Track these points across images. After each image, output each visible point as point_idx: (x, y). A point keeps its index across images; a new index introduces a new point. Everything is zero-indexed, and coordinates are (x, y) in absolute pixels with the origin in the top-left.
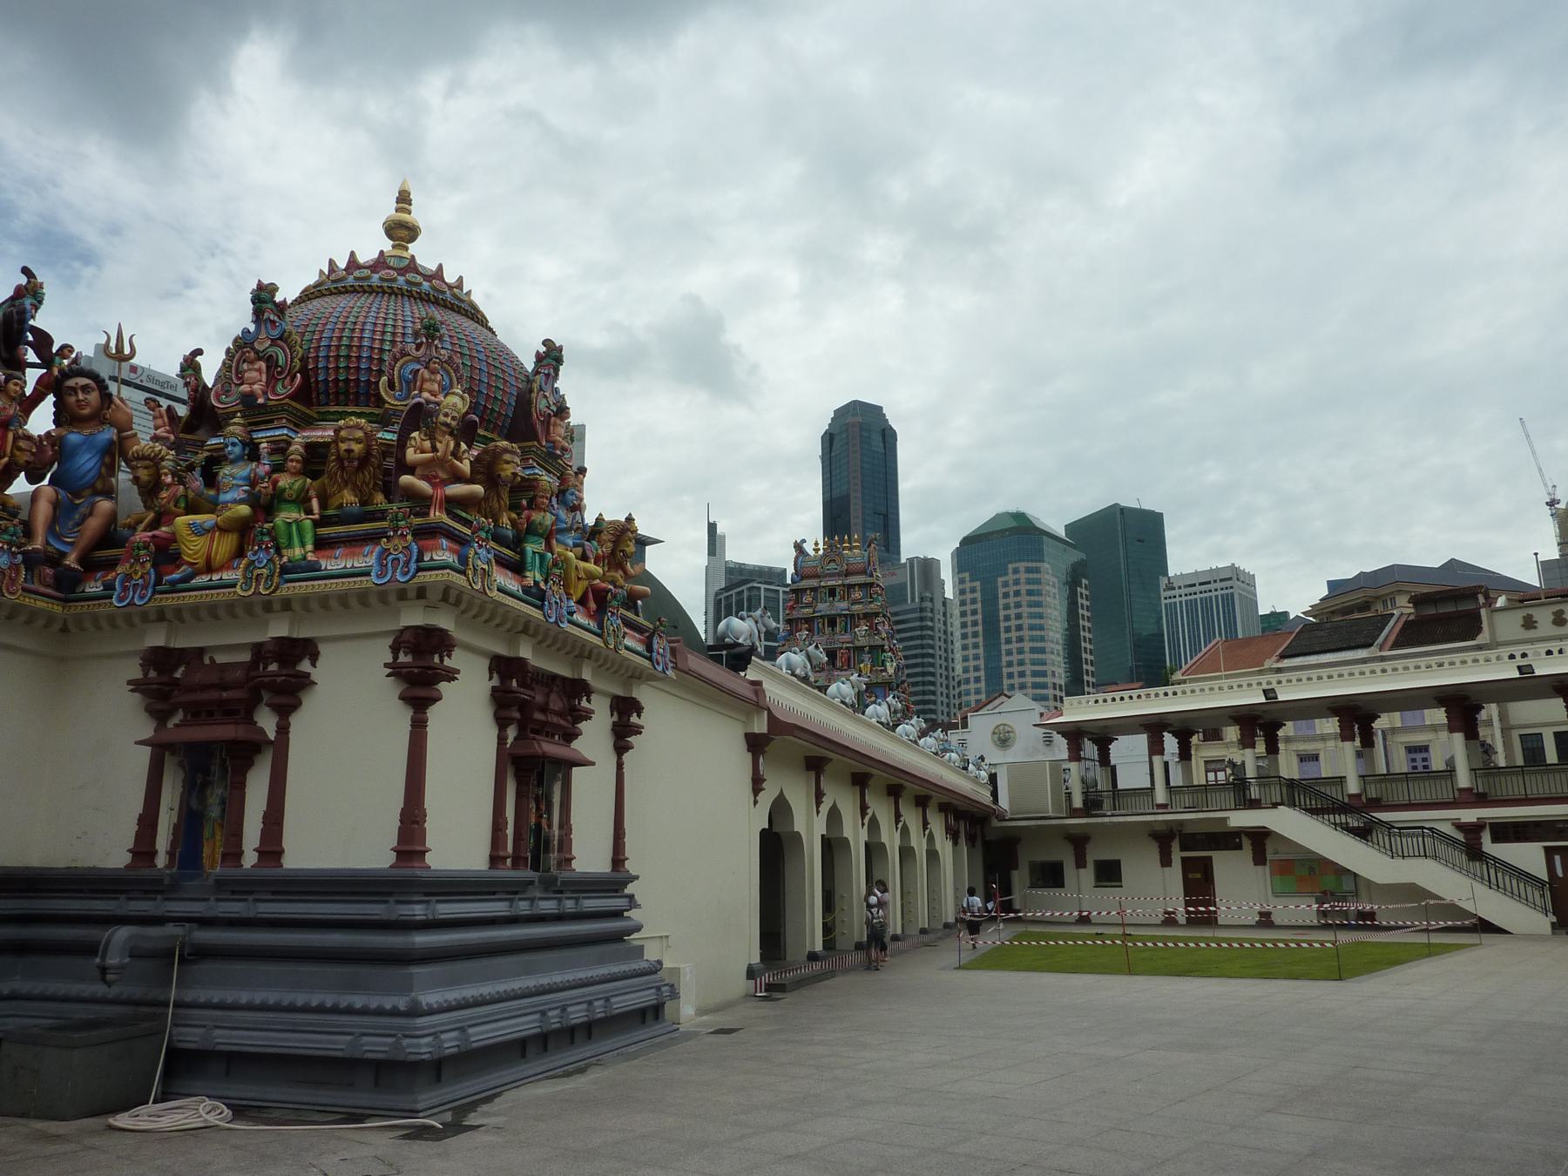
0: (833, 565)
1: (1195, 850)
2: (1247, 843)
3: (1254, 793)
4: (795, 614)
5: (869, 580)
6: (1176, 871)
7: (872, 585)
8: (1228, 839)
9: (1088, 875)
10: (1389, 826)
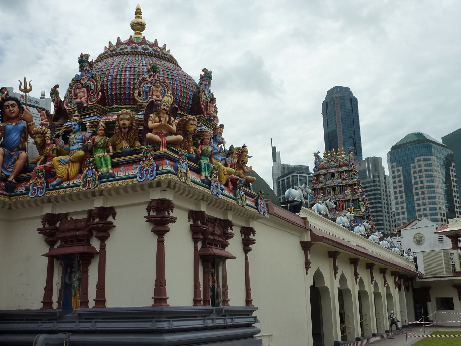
0: (333, 163)
4: (316, 186)
5: (350, 169)
7: (351, 171)
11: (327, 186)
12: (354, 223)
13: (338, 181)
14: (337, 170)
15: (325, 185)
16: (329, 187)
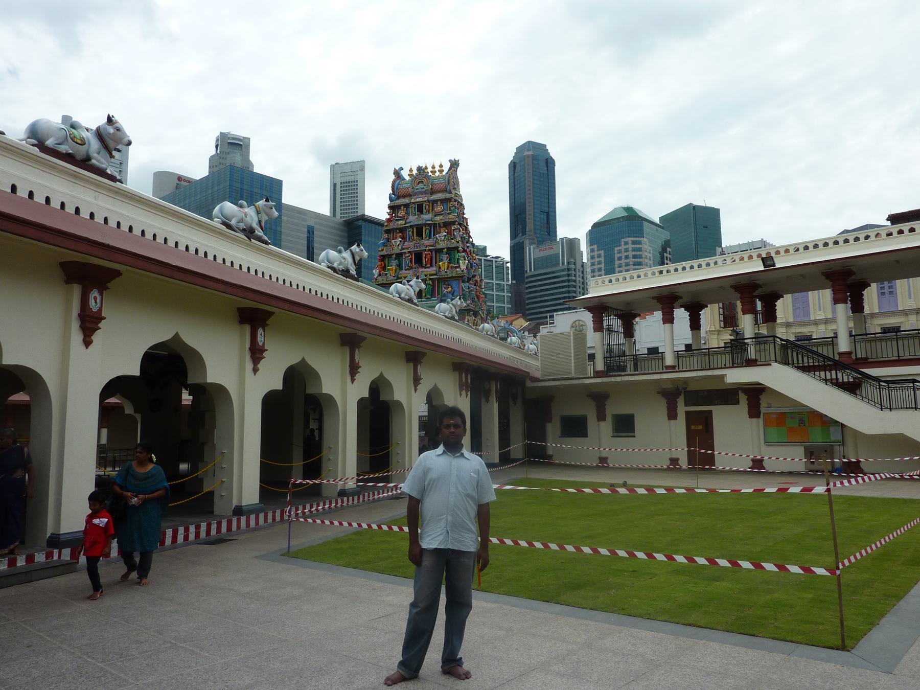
0: (421, 186)
1: (698, 405)
2: (743, 399)
3: (752, 353)
6: (680, 425)
7: (450, 200)
9: (607, 427)
10: (877, 379)
13: (427, 217)
16: (411, 226)
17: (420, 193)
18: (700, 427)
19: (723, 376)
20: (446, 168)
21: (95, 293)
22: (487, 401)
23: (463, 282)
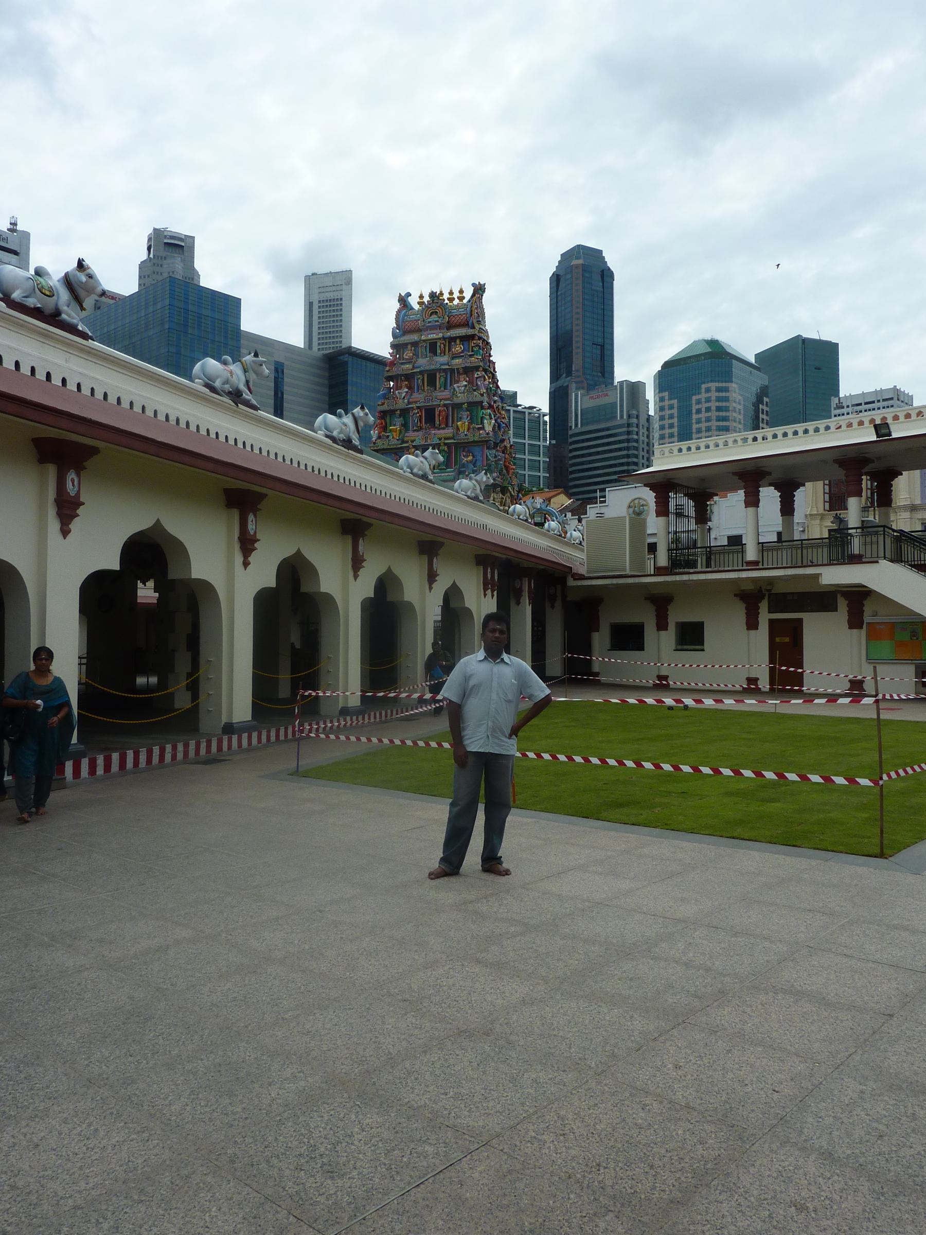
0: (434, 318)
1: (783, 610)
2: (842, 604)
5: (470, 332)
7: (472, 337)
8: (823, 600)
9: (668, 638)
11: (418, 370)
12: (467, 456)
13: (442, 360)
14: (441, 335)
15: (414, 368)
16: (421, 372)
17: (433, 328)
18: (787, 640)
19: (817, 577)
20: (468, 295)
21: (72, 475)
22: (518, 603)
23: (488, 448)
